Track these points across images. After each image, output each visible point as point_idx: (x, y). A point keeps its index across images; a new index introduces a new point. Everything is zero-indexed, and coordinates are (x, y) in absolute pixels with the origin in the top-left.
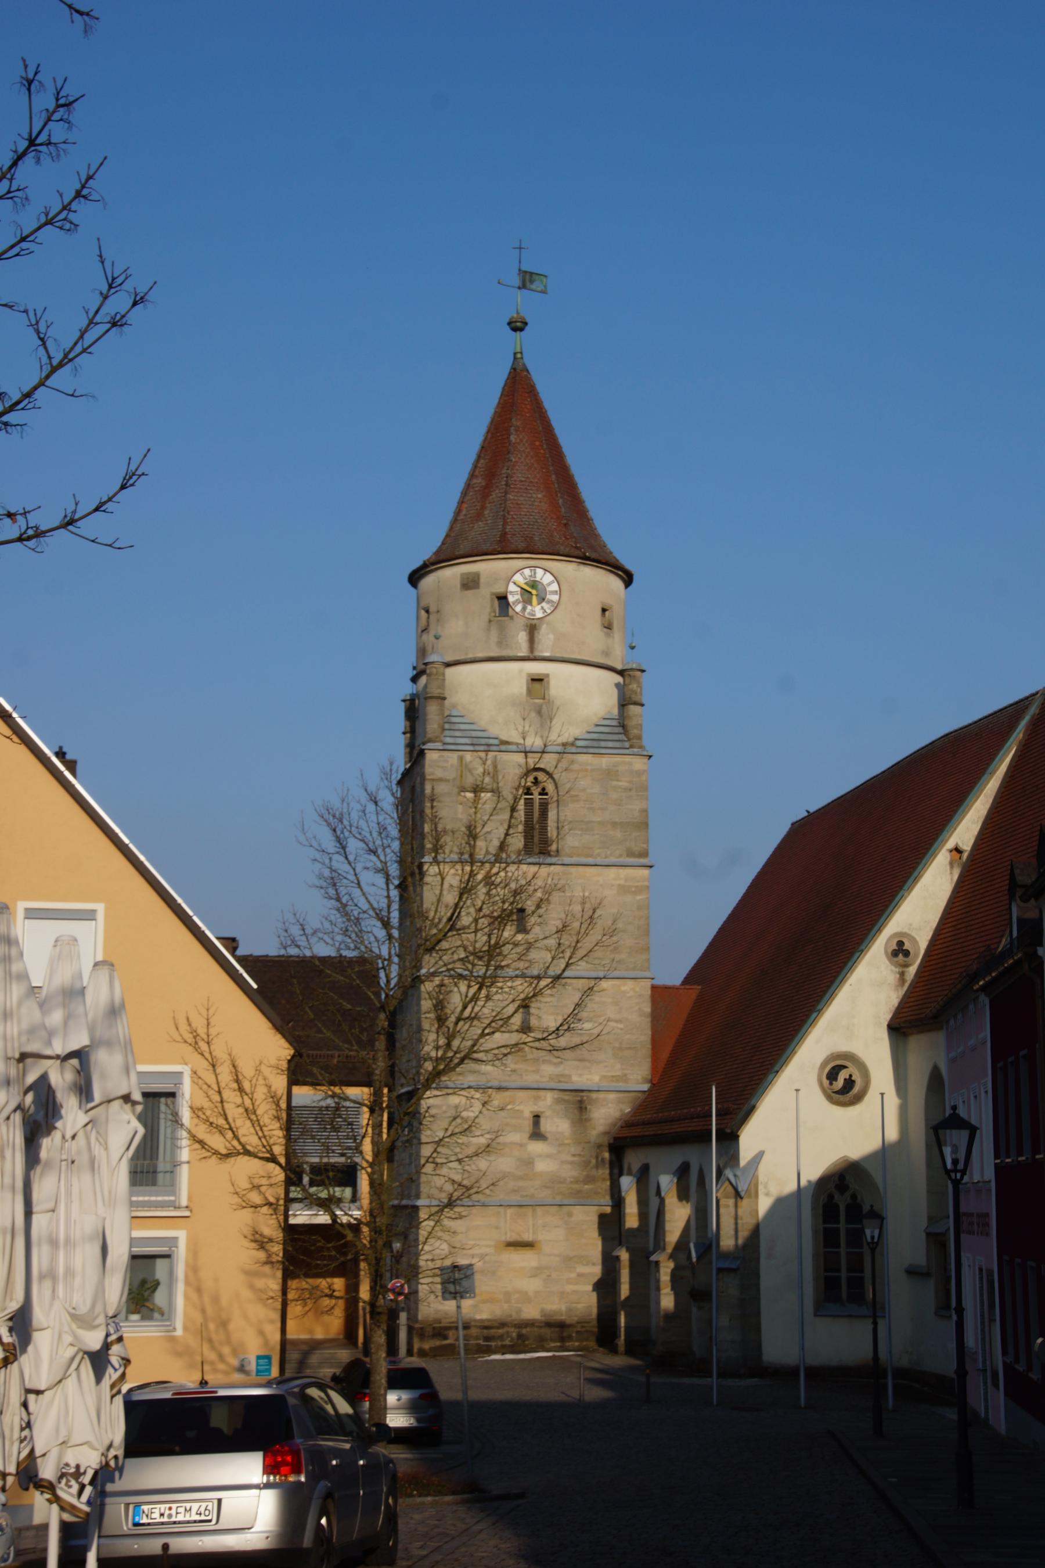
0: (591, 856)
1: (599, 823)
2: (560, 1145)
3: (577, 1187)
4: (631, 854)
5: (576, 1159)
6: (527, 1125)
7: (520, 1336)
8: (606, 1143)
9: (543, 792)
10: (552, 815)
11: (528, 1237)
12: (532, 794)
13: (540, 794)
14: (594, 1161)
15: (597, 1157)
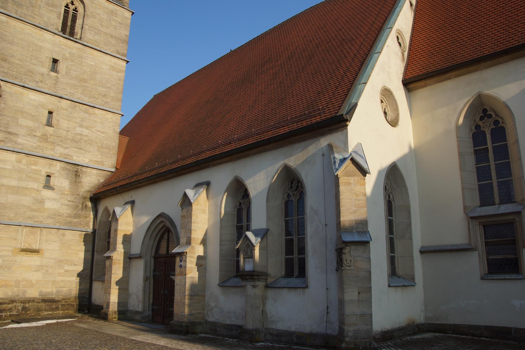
0: (98, 46)
1: (104, 32)
2: (62, 194)
3: (69, 219)
4: (118, 52)
5: (70, 203)
6: (43, 179)
7: (24, 308)
8: (89, 197)
9: (75, 10)
10: (79, 22)
11: (35, 247)
12: (69, 8)
13: (73, 10)
14: (81, 206)
15: (83, 204)
